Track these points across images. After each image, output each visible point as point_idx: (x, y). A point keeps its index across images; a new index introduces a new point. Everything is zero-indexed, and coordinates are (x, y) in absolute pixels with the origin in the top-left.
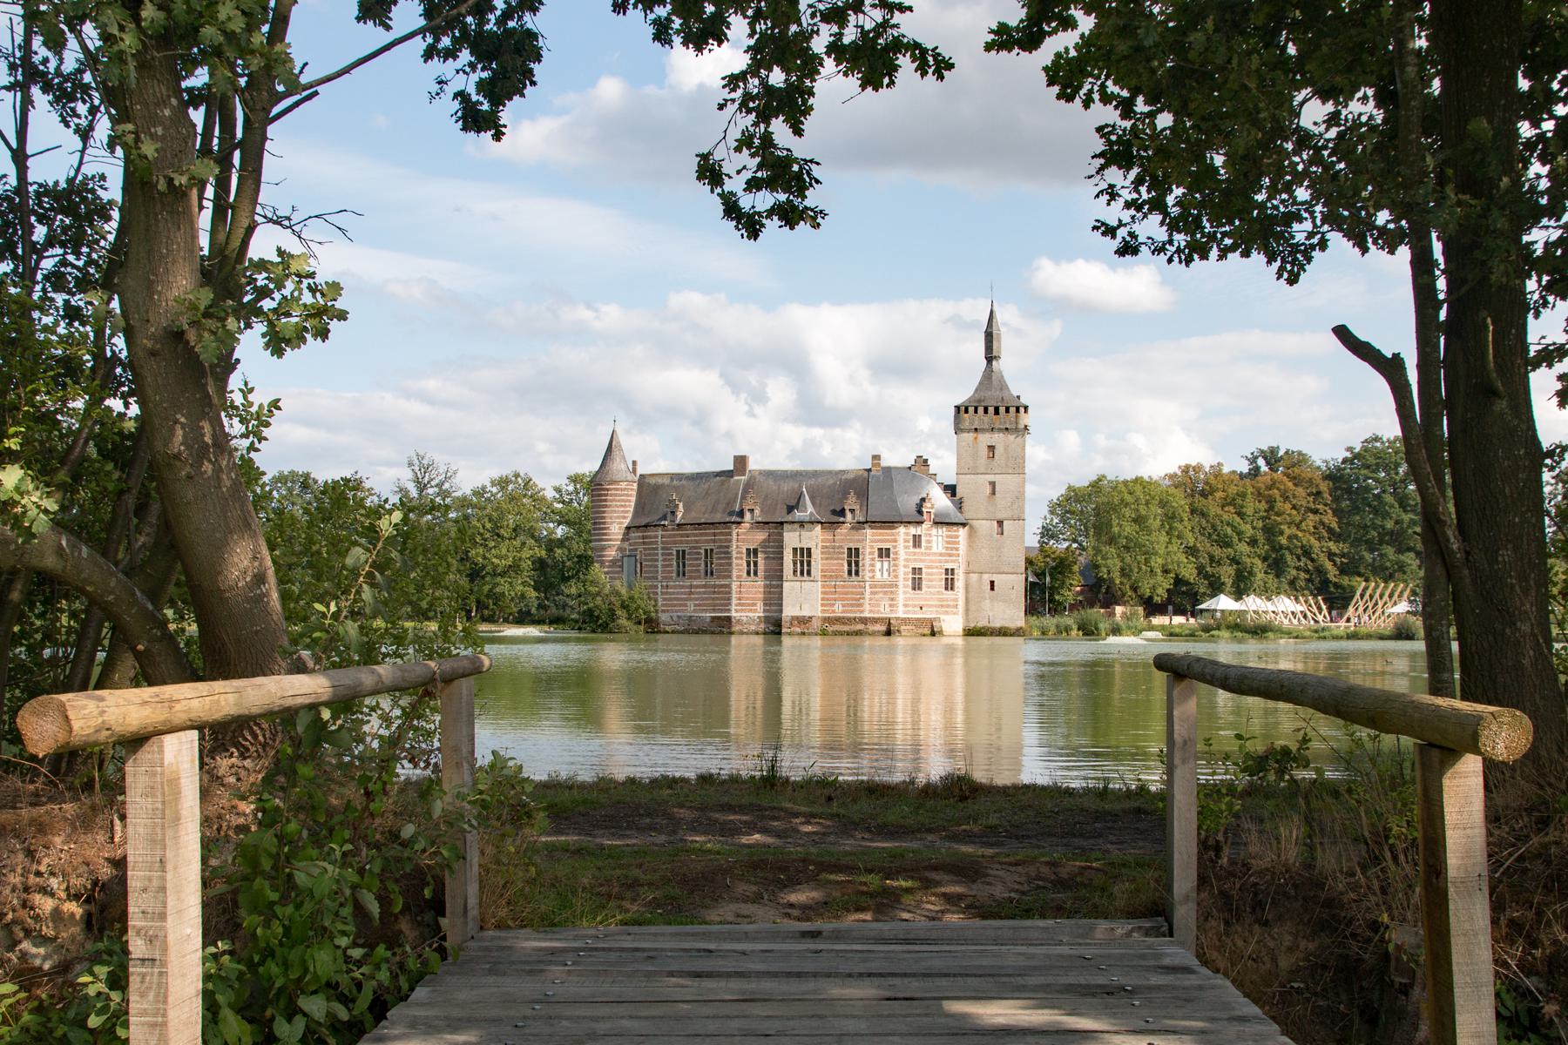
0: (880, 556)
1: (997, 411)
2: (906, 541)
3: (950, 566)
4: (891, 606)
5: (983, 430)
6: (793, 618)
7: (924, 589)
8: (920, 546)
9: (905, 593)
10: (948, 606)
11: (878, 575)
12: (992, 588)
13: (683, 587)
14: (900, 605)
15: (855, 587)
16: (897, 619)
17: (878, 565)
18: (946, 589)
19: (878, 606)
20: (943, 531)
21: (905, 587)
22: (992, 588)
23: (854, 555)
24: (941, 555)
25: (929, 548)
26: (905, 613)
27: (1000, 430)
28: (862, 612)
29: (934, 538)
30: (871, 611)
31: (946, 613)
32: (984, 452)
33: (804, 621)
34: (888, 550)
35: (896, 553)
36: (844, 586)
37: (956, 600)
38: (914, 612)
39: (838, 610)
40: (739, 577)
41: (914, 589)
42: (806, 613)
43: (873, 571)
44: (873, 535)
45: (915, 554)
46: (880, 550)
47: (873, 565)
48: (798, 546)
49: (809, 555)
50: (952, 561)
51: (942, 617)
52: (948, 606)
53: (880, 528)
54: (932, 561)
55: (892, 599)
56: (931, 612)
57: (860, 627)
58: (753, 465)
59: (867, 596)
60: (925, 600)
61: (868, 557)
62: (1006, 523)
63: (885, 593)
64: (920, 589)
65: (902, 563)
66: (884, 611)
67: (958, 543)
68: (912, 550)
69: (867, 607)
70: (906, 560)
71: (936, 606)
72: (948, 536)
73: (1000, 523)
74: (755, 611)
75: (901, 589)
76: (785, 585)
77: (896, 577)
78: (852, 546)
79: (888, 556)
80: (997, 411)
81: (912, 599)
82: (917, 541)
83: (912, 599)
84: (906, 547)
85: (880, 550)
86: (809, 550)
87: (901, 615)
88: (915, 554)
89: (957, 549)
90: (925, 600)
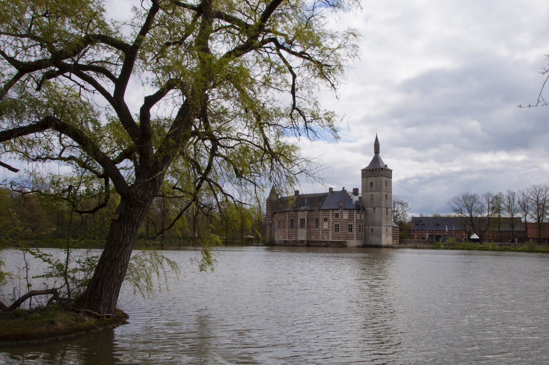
0: (325, 221)
1: (373, 171)
2: (332, 215)
3: (350, 224)
4: (328, 237)
5: (369, 177)
6: (300, 241)
7: (340, 231)
8: (338, 217)
9: (332, 233)
10: (350, 237)
11: (324, 227)
12: (372, 231)
13: (281, 231)
14: (330, 237)
15: (317, 231)
16: (329, 241)
17: (324, 223)
18: (349, 231)
19: (324, 237)
20: (347, 212)
21: (332, 230)
22: (372, 231)
23: (317, 220)
24: (347, 220)
25: (342, 218)
26: (332, 239)
27: (374, 177)
28: (319, 239)
29: (344, 214)
30: (322, 239)
31: (349, 240)
32: (369, 184)
33: (302, 242)
34: (327, 219)
35: (329, 220)
36: (314, 231)
37: (353, 235)
38: (336, 239)
39: (313, 238)
40: (289, 228)
41: (336, 231)
42: (303, 239)
43: (322, 226)
44: (323, 214)
45: (336, 220)
46: (325, 219)
47: (322, 224)
48: (301, 218)
49: (304, 221)
50: (351, 222)
51: (347, 241)
52: (350, 237)
53: (325, 211)
54: (343, 222)
55: (328, 235)
56: (343, 239)
57: (319, 244)
58: (300, 193)
59: (321, 234)
60: (340, 235)
61: (321, 221)
62: (376, 208)
63: (326, 233)
64: (338, 231)
65: (331, 223)
66: (326, 239)
67: (354, 216)
68: (335, 218)
69: (320, 237)
70: (332, 222)
71: (346, 237)
72: (349, 214)
73: (374, 209)
74: (292, 238)
75: (330, 232)
76: (299, 230)
77: (329, 227)
78: (317, 217)
79: (327, 221)
80: (373, 171)
81: (335, 235)
82: (337, 215)
83: (335, 235)
84: (332, 218)
85: (325, 219)
86: (304, 219)
87: (331, 240)
88: (336, 220)
89: (353, 218)
90: (340, 235)
